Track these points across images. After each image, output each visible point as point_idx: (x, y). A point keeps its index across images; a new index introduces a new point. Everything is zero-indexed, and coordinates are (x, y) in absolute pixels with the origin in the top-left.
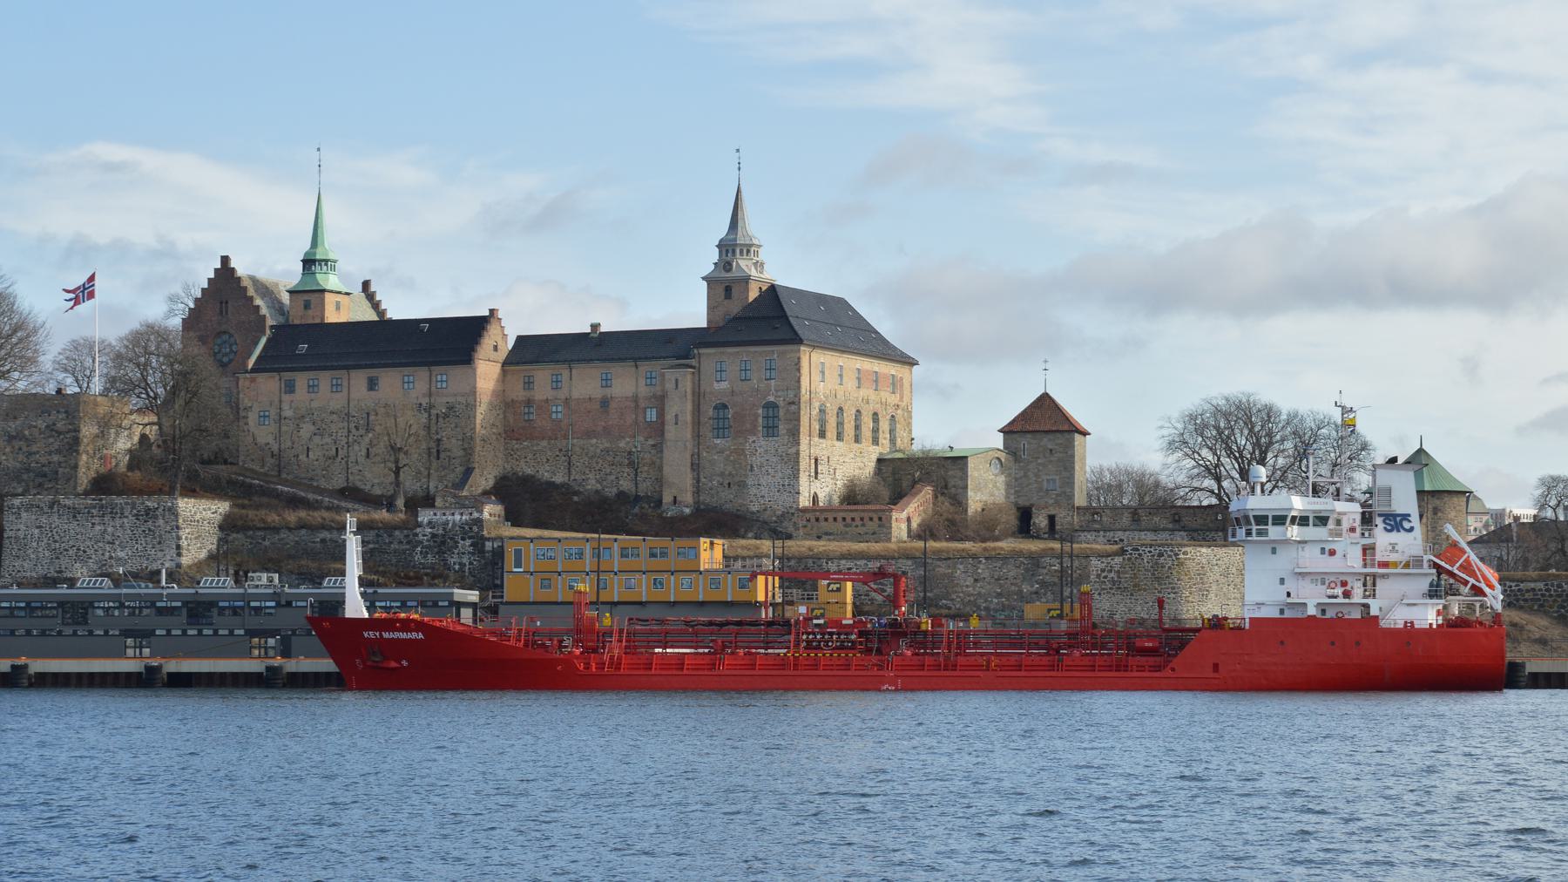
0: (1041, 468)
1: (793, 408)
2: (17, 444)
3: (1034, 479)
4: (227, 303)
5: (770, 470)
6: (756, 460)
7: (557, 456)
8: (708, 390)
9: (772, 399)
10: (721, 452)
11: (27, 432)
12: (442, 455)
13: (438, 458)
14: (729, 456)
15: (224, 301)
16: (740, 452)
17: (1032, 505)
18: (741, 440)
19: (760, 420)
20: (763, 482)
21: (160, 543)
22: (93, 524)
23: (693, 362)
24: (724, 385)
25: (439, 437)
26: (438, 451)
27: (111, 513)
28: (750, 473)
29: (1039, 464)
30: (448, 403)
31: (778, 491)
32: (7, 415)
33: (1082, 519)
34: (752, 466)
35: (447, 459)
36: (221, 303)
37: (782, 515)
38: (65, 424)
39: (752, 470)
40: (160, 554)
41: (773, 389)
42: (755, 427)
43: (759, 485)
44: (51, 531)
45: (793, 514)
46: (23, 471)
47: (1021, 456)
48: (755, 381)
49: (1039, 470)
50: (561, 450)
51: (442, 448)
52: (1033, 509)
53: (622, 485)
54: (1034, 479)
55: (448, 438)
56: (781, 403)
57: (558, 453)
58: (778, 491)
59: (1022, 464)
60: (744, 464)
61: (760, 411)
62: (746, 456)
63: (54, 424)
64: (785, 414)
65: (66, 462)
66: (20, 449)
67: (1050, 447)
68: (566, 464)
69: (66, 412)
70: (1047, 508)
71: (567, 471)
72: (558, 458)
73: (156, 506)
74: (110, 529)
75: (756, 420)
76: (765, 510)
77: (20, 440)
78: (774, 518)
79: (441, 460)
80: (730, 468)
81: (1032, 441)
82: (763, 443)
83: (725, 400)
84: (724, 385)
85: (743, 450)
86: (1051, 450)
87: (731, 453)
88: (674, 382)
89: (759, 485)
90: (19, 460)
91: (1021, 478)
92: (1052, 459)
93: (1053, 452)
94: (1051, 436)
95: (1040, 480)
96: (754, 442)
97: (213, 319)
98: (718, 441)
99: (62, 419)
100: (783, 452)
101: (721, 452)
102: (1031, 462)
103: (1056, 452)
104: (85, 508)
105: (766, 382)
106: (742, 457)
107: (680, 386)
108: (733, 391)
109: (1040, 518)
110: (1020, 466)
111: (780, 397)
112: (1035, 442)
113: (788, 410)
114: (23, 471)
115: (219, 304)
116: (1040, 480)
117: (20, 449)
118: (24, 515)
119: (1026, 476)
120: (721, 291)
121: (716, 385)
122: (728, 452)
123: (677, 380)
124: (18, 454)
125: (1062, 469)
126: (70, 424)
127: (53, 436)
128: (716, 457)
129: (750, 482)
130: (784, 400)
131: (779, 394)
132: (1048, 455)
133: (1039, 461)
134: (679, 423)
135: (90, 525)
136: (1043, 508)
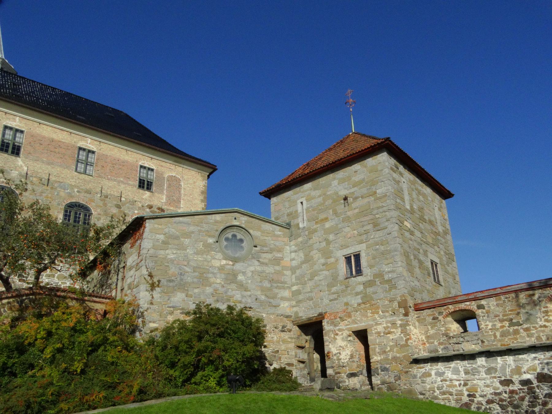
0: (331, 237)
3: (322, 261)
17: (322, 316)
29: (328, 231)
33: (432, 332)
47: (298, 224)
49: (328, 242)
52: (325, 323)
54: (322, 261)
59: (300, 239)
67: (343, 193)
70: (350, 316)
81: (313, 193)
86: (345, 199)
91: (299, 267)
92: (349, 213)
93: (350, 200)
94: (341, 174)
95: (332, 260)
102: (315, 231)
103: (356, 199)
109: (340, 342)
110: (296, 245)
112: (317, 193)
116: (332, 260)
119: (308, 260)
125: (370, 227)
132: (341, 207)
133: (327, 225)
136: (342, 319)
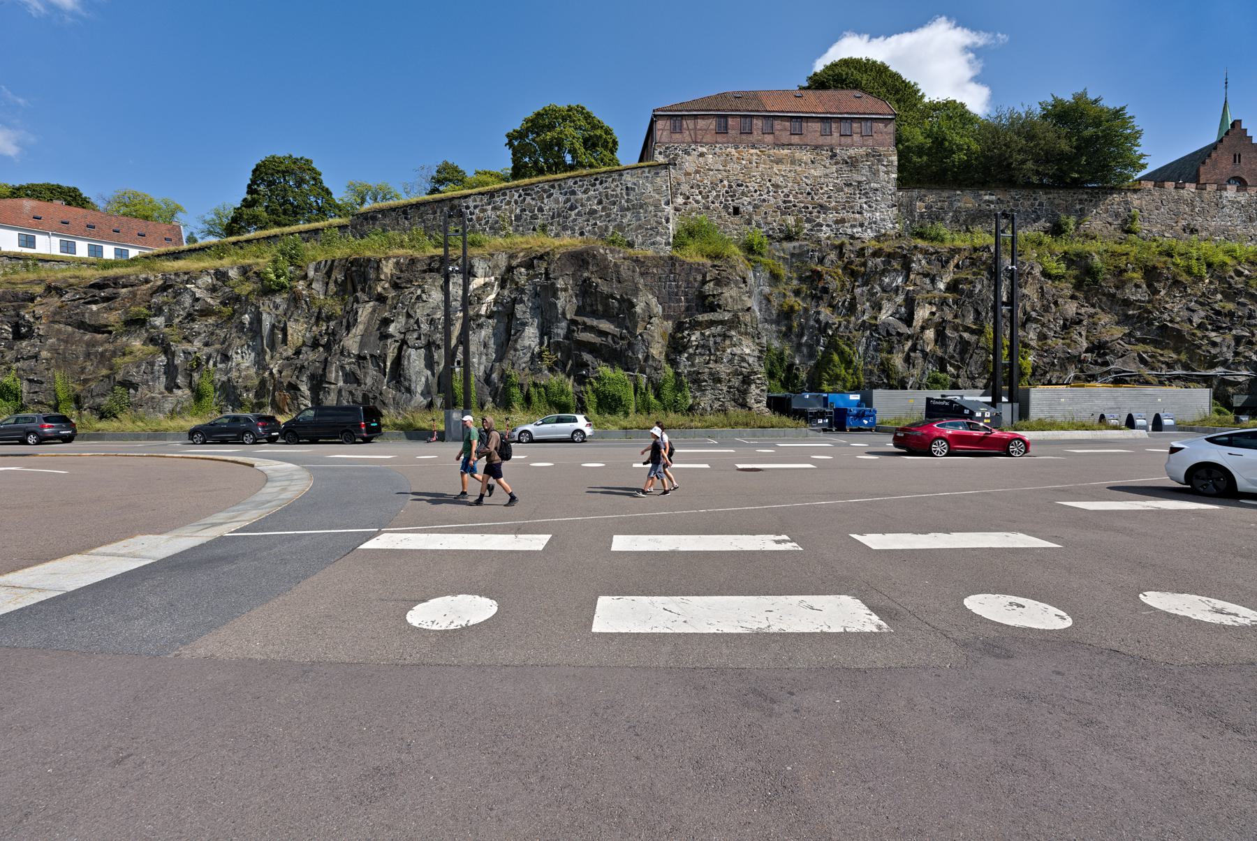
4: (1239, 156)
36: (1235, 156)
115: (1233, 157)
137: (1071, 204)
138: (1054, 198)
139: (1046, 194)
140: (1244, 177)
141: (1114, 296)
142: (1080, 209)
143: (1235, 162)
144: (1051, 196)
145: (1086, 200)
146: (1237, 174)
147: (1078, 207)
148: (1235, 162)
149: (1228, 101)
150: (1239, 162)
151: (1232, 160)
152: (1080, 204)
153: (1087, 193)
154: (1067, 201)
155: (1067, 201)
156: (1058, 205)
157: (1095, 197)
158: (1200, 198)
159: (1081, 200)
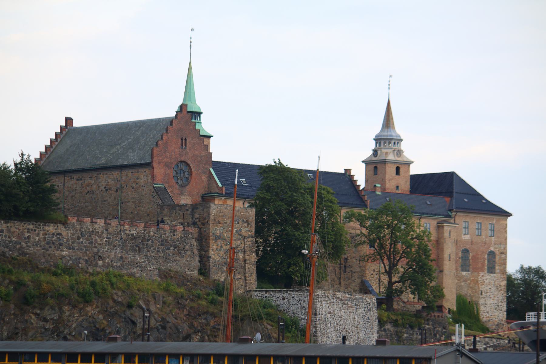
1: (503, 256)
2: (220, 242)
4: (186, 140)
5: (491, 295)
6: (484, 288)
7: (372, 274)
8: (459, 240)
9: (492, 249)
10: (465, 281)
11: (225, 234)
12: (348, 269)
13: (345, 272)
14: (470, 284)
15: (184, 138)
16: (476, 282)
18: (476, 274)
19: (486, 262)
20: (489, 301)
21: (372, 329)
22: (350, 312)
23: (452, 220)
24: (467, 237)
25: (346, 257)
26: (345, 267)
27: (356, 305)
28: (481, 296)
30: (351, 233)
31: (496, 309)
32: (215, 220)
34: (482, 292)
35: (350, 273)
36: (182, 139)
37: (497, 325)
38: (246, 231)
39: (481, 294)
40: (372, 336)
41: (493, 242)
42: (483, 265)
43: (486, 304)
44: (335, 317)
45: (503, 325)
46: (223, 264)
48: (484, 237)
50: (374, 271)
51: (348, 264)
53: (410, 298)
55: (351, 258)
56: (497, 253)
57: (372, 273)
58: (496, 309)
60: (478, 290)
61: (486, 256)
62: (478, 285)
63: (240, 230)
64: (499, 260)
65: (249, 260)
66: (221, 247)
68: (377, 280)
69: (247, 222)
71: (378, 285)
72: (372, 276)
73: (370, 302)
74: (356, 317)
75: (484, 261)
76: (489, 321)
77: (222, 240)
78: (494, 327)
79: (347, 273)
80: (470, 292)
82: (488, 277)
83: (467, 247)
84: (467, 237)
85: (477, 281)
87: (471, 282)
88: (448, 232)
89: (486, 304)
90: (221, 255)
96: (483, 276)
97: (176, 150)
98: (464, 273)
99: (245, 227)
100: (498, 284)
101: (465, 281)
104: (346, 300)
105: (489, 238)
106: (477, 285)
107: (452, 235)
108: (472, 242)
111: (496, 248)
113: (500, 257)
114: (223, 264)
115: (180, 141)
117: (221, 247)
118: (324, 303)
120: (372, 167)
121: (463, 237)
122: (469, 281)
123: (450, 231)
124: (220, 250)
126: (249, 231)
127: (240, 239)
128: (463, 284)
129: (481, 302)
130: (499, 251)
131: (496, 246)
134: (451, 260)
135: (349, 314)
137: (22, 232)
138: (11, 227)
139: (6, 223)
140: (189, 162)
141: (38, 315)
142: (28, 236)
143: (182, 145)
144: (9, 225)
145: (32, 230)
146: (183, 159)
147: (27, 235)
148: (182, 145)
149: (191, 62)
150: (186, 146)
151: (180, 144)
152: (28, 232)
153: (33, 224)
154: (19, 230)
155: (19, 230)
156: (14, 232)
157: (38, 228)
158: (107, 230)
159: (28, 229)
